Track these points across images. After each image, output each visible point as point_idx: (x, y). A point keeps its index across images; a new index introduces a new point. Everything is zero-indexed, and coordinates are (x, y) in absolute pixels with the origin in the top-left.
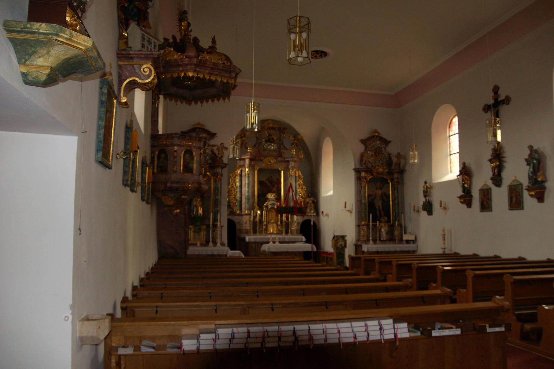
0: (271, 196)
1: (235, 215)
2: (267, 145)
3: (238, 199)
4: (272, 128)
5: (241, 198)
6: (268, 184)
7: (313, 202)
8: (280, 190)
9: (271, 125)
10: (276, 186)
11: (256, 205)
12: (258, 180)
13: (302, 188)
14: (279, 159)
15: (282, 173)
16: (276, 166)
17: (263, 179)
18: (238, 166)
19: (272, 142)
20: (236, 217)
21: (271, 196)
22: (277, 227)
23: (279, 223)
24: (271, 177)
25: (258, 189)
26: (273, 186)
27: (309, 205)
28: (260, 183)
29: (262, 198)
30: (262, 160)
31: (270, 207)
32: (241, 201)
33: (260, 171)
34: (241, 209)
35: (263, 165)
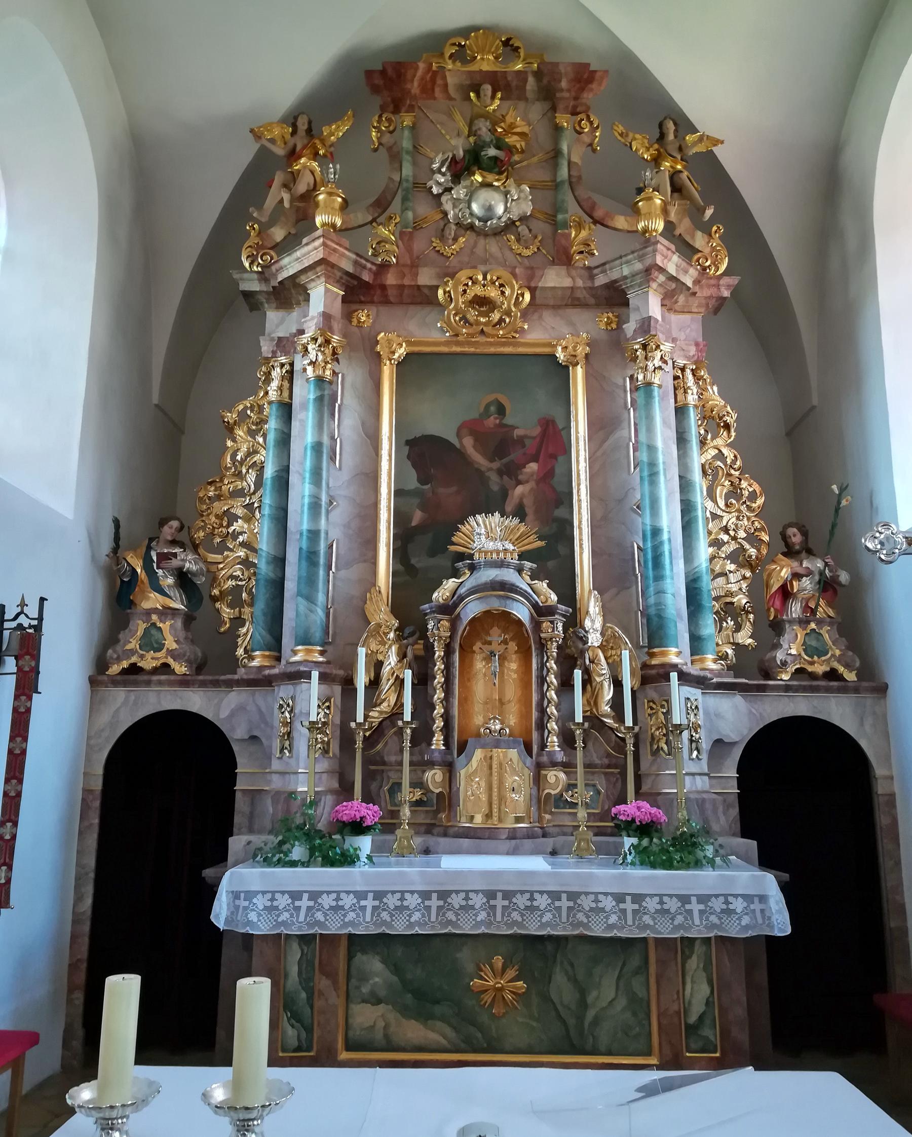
0: (488, 535)
1: (230, 684)
2: (460, 192)
3: (263, 567)
4: (499, 83)
5: (280, 561)
6: (479, 459)
7: (828, 586)
8: (565, 499)
9: (486, 63)
10: (533, 467)
11: (381, 613)
12: (400, 426)
13: (735, 492)
14: (554, 278)
15: (579, 374)
16: (536, 335)
17: (441, 420)
18: (266, 348)
19: (496, 166)
20: (234, 698)
21: (488, 535)
22: (538, 780)
23: (554, 742)
24: (501, 410)
25: (399, 493)
26: (512, 472)
27: (795, 610)
28: (420, 451)
29: (426, 544)
30: (424, 298)
31: (472, 609)
32: (278, 586)
33: (415, 368)
34: (275, 645)
35: (433, 332)
